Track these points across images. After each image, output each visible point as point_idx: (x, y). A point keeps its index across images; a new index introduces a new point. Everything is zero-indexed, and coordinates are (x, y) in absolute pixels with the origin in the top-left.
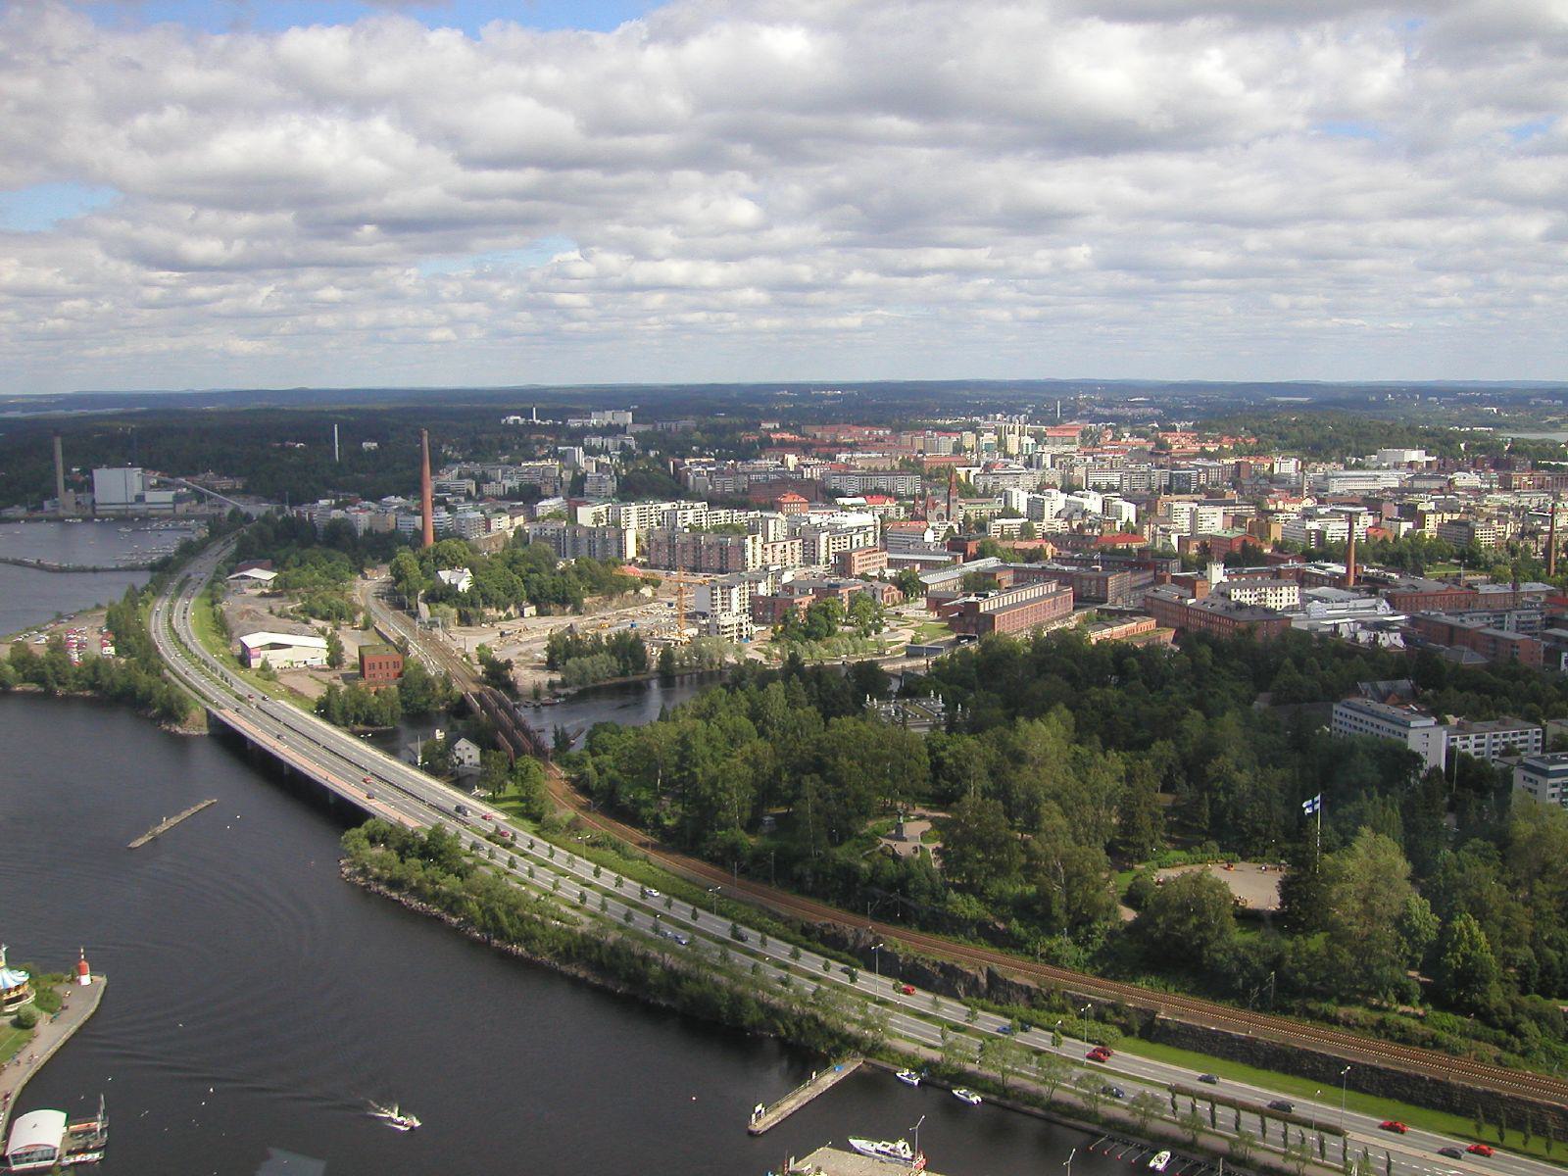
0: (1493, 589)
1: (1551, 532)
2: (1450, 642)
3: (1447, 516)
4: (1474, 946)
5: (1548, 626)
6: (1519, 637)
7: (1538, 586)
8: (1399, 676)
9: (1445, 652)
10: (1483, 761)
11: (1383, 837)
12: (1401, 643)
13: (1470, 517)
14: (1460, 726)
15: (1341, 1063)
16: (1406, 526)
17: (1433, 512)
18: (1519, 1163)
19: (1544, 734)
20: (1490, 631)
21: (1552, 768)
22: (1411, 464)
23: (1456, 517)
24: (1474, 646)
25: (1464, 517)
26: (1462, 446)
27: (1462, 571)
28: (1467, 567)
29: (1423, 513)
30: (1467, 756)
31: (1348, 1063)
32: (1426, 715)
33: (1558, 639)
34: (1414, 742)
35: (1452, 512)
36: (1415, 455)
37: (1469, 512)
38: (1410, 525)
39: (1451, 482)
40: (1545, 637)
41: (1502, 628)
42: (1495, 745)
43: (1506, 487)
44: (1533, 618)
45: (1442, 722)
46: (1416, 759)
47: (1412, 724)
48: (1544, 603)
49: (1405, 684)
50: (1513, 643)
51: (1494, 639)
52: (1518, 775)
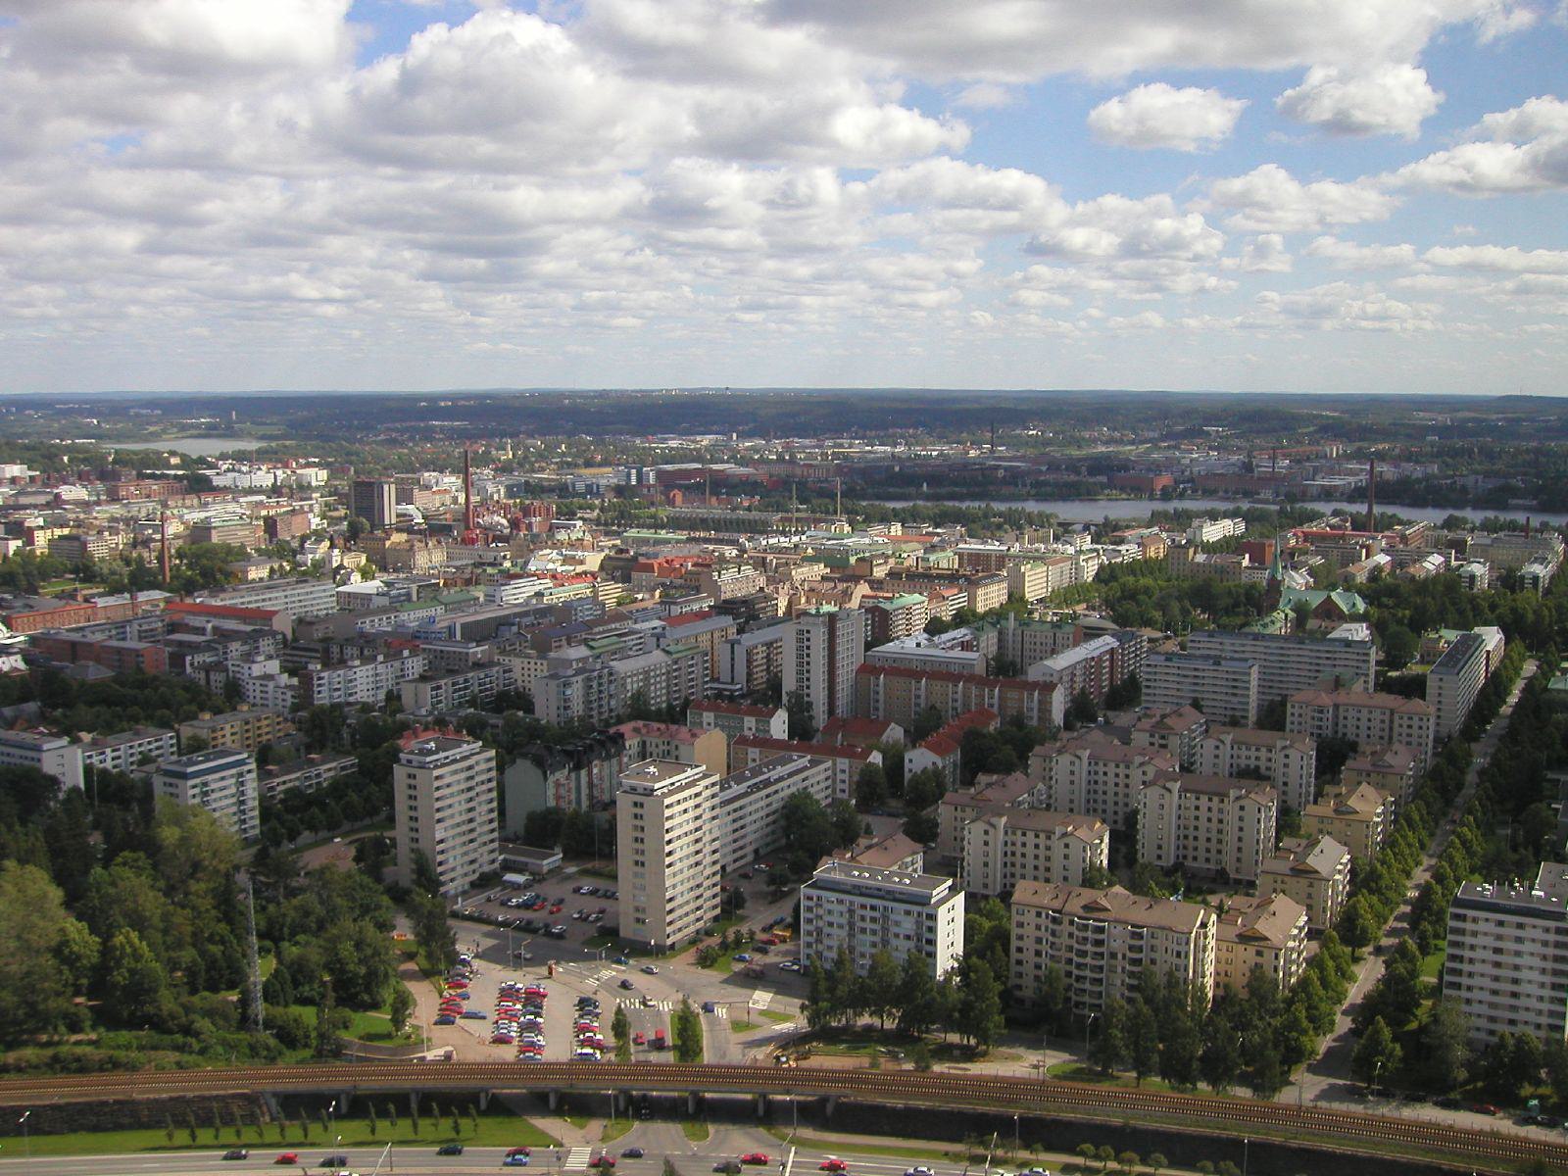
0: (111, 601)
1: (162, 540)
2: (74, 659)
3: (58, 532)
4: (137, 956)
5: (171, 632)
6: (142, 645)
7: (156, 594)
8: (24, 699)
9: (69, 669)
10: (122, 774)
11: (30, 868)
12: (22, 665)
13: (81, 530)
14: (94, 743)
15: (18, 1111)
16: (14, 545)
17: (42, 528)
18: (209, 1158)
19: (178, 737)
20: (114, 643)
21: (190, 770)
22: (13, 480)
23: (66, 531)
24: (98, 660)
25: (74, 531)
26: (66, 459)
27: (78, 585)
28: (83, 581)
29: (31, 530)
30: (105, 771)
31: (26, 1108)
32: (58, 735)
33: (180, 643)
34: (49, 765)
35: (62, 526)
36: (15, 470)
37: (79, 526)
38: (19, 543)
39: (57, 496)
40: (168, 643)
41: (124, 639)
42: (132, 755)
43: (114, 498)
44: (154, 626)
45: (75, 741)
46: (53, 781)
47: (45, 747)
48: (163, 611)
49: (32, 707)
50: (137, 653)
51: (119, 651)
52: (158, 782)
